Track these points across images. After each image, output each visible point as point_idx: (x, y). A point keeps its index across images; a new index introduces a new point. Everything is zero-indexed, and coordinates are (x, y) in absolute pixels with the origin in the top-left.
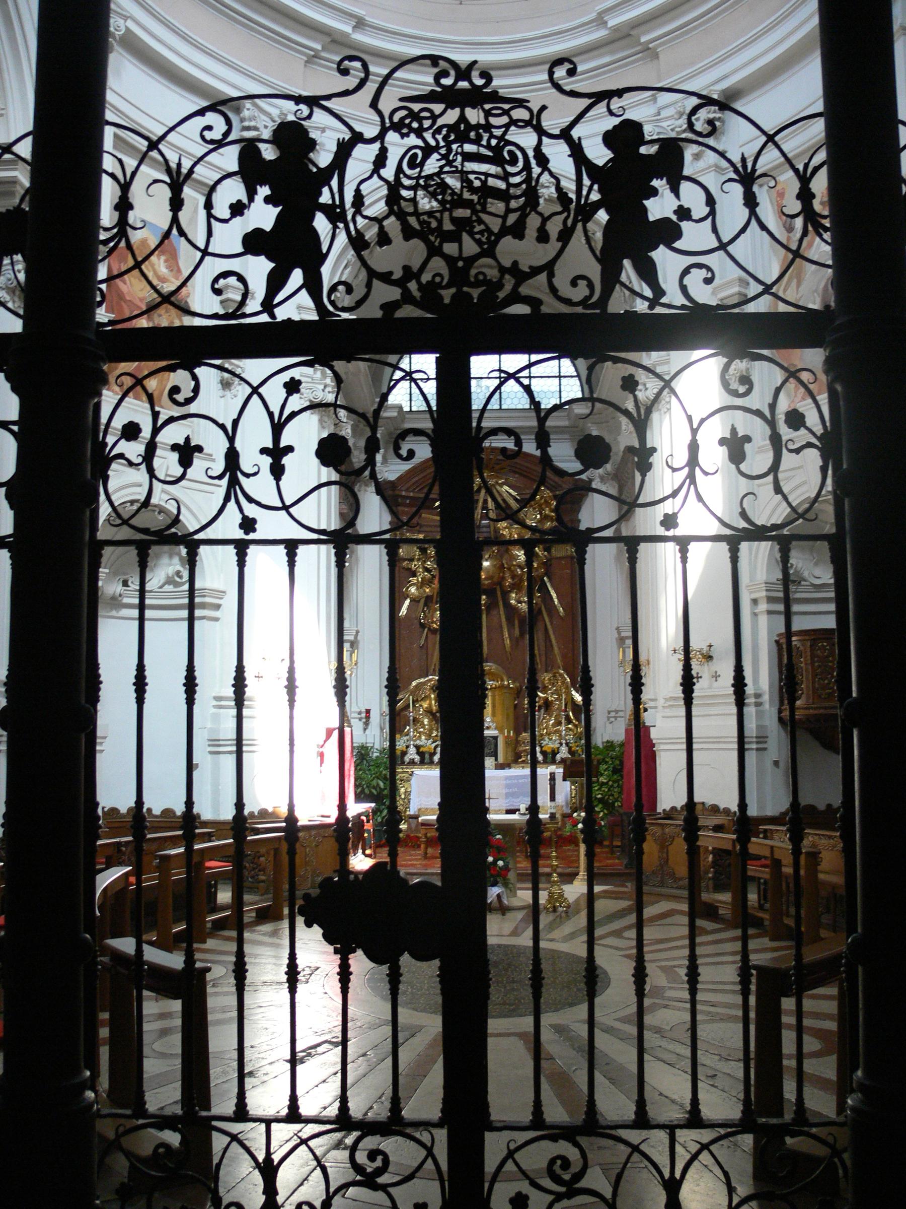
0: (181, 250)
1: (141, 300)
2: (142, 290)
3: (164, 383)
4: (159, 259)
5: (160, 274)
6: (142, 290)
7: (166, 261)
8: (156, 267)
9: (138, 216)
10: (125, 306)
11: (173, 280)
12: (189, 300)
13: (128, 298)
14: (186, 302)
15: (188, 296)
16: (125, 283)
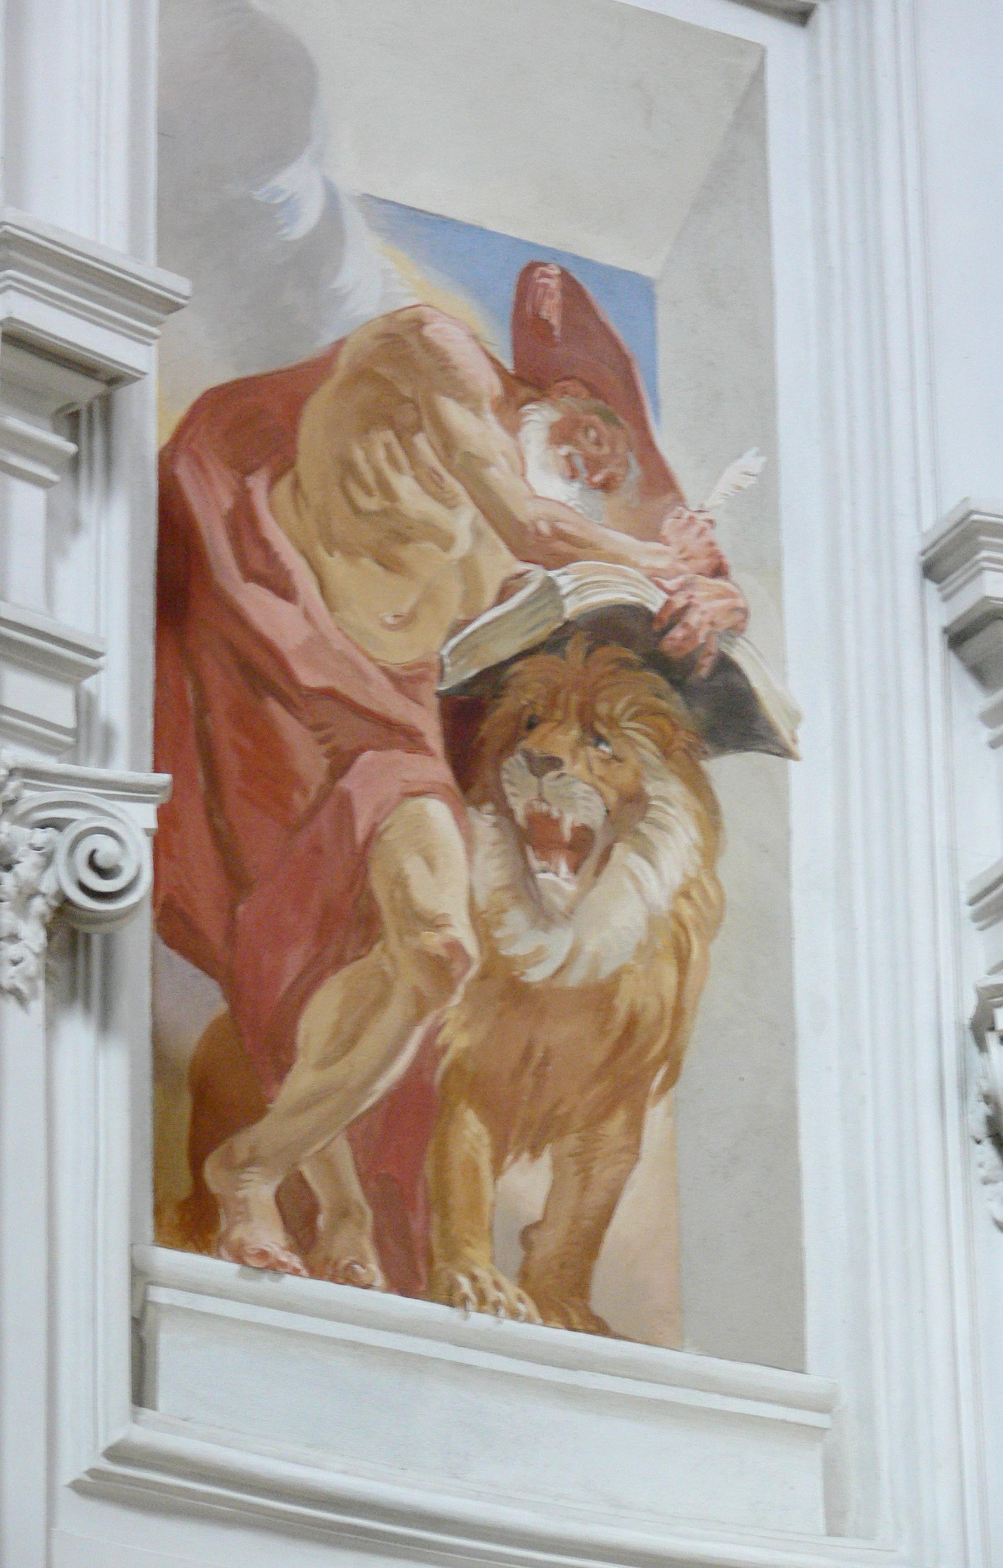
0: (665, 355)
1: (404, 682)
2: (406, 621)
3: (603, 1174)
4: (513, 429)
5: (525, 511)
6: (406, 621)
7: (561, 434)
8: (499, 475)
9: (353, 178)
10: (291, 729)
11: (623, 541)
12: (738, 655)
13: (309, 677)
14: (726, 665)
15: (736, 630)
16: (286, 592)
